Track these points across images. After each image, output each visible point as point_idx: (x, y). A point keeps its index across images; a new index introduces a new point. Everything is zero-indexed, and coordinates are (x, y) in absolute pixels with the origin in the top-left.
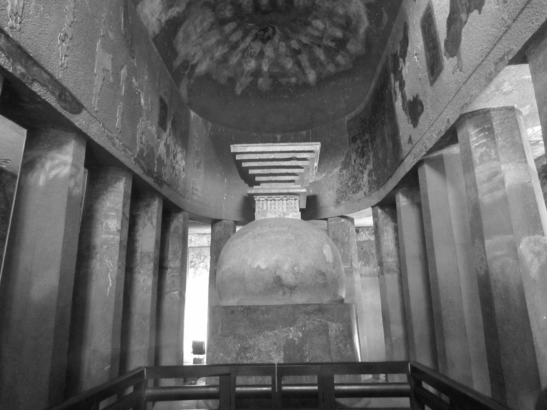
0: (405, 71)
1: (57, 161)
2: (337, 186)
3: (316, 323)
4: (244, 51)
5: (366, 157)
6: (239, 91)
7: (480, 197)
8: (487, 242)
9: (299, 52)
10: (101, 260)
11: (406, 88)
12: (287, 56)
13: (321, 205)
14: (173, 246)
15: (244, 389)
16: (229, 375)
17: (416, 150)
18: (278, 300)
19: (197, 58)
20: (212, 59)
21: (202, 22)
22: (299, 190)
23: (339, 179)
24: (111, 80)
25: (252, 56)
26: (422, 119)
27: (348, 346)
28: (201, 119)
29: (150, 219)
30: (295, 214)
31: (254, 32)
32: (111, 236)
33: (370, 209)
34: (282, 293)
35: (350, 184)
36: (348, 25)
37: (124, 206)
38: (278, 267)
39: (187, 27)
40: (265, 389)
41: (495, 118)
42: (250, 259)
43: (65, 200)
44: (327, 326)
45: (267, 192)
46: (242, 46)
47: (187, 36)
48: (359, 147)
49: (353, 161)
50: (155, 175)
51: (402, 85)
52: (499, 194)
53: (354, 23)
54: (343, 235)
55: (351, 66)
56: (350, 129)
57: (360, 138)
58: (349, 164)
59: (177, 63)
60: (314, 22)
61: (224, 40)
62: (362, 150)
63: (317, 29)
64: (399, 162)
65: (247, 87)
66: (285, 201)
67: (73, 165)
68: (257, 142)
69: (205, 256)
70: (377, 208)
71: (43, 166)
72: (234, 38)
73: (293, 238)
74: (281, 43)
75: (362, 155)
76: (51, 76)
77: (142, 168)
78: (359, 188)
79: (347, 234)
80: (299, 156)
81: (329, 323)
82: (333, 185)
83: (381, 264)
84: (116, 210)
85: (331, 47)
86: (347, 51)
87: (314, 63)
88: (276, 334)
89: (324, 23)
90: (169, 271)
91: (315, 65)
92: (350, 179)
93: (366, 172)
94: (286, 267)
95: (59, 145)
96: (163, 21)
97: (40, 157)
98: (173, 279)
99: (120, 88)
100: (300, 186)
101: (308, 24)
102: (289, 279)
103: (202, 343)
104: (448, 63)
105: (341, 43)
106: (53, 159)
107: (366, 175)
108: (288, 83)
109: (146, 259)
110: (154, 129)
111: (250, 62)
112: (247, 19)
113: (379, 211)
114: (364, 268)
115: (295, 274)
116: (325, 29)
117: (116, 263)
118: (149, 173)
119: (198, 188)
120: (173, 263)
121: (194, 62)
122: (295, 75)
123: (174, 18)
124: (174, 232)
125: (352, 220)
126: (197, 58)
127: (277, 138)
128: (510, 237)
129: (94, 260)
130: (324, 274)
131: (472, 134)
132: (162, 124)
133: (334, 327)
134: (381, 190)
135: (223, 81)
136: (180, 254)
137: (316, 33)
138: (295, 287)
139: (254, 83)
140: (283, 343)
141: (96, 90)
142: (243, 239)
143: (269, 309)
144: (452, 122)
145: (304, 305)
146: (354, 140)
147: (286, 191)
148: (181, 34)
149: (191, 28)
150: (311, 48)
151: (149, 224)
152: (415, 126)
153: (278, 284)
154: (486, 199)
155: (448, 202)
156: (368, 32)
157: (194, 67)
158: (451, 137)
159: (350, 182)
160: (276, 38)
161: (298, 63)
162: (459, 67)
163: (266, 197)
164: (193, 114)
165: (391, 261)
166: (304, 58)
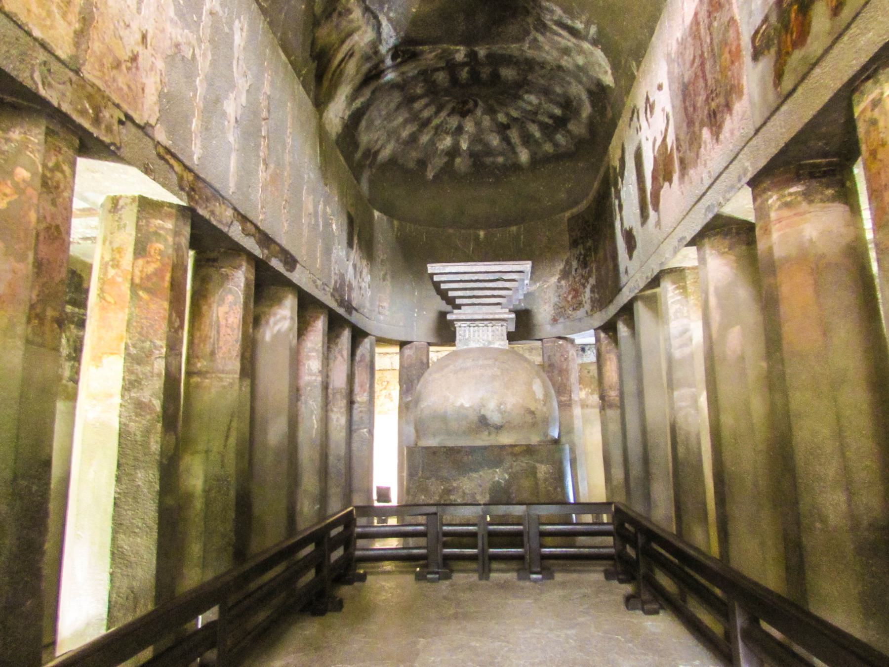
1: (278, 317)
2: (555, 299)
3: (524, 465)
4: (437, 128)
5: (588, 269)
6: (430, 175)
7: (672, 350)
8: (676, 394)
9: (506, 127)
10: (306, 402)
11: (624, 213)
12: (492, 131)
13: (535, 322)
14: (361, 376)
15: (450, 528)
16: (435, 514)
17: (631, 284)
18: (483, 440)
19: (380, 143)
20: (397, 140)
21: (388, 104)
22: (506, 316)
23: (556, 291)
24: (313, 222)
25: (447, 133)
26: (635, 253)
27: (559, 489)
28: (385, 218)
29: (340, 352)
30: (502, 343)
31: (450, 106)
32: (314, 378)
33: (592, 332)
34: (486, 433)
35: (569, 299)
36: (569, 105)
37: (323, 346)
38: (484, 406)
39: (373, 112)
40: (471, 528)
41: (689, 277)
42: (452, 397)
43: (288, 352)
44: (535, 468)
45: (469, 317)
46: (436, 122)
47: (371, 123)
48: (581, 254)
50: (346, 303)
51: (621, 207)
52: (687, 350)
53: (574, 103)
54: (561, 361)
55: (573, 148)
56: (571, 230)
57: (583, 243)
58: (569, 273)
59: (358, 155)
60: (526, 96)
61: (414, 117)
62: (584, 259)
63: (530, 103)
64: (617, 289)
65: (442, 168)
66: (490, 328)
67: (292, 318)
68: (460, 262)
69: (388, 382)
70: (600, 331)
71: (267, 323)
72: (426, 114)
73: (499, 373)
74: (485, 116)
75: (584, 264)
77: (336, 300)
78: (580, 304)
81: (538, 465)
82: (550, 298)
83: (602, 397)
84: (317, 351)
85: (547, 123)
86: (569, 132)
87: (527, 139)
89: (540, 100)
90: (356, 406)
91: (528, 142)
92: (569, 293)
95: (279, 301)
96: (346, 117)
97: (264, 313)
98: (361, 415)
99: (318, 225)
100: (507, 310)
101: (520, 97)
102: (495, 418)
103: (388, 489)
104: (652, 213)
105: (561, 123)
106: (275, 314)
108: (493, 163)
110: (342, 253)
111: (445, 139)
112: (443, 93)
113: (602, 335)
114: (590, 397)
115: (501, 412)
116: (540, 104)
117: (319, 404)
118: (341, 303)
119: (385, 304)
120: (361, 397)
121: (376, 149)
122: (501, 154)
123: (358, 110)
124: (360, 361)
125: (572, 341)
126: (380, 143)
127: (477, 237)
128: (694, 390)
129: (299, 403)
130: (532, 413)
131: (668, 290)
132: (350, 244)
133: (543, 470)
134: (603, 311)
135: (412, 165)
136: (368, 385)
137: (529, 108)
138: (501, 427)
139: (449, 164)
140: (489, 485)
141: (304, 240)
143: (473, 450)
144: (655, 273)
145: (512, 446)
146: (574, 244)
147: (491, 317)
148: (363, 123)
149: (376, 113)
150: (523, 122)
151: (340, 357)
152: (631, 257)
153: (483, 422)
154: (677, 354)
155: (658, 343)
156: (591, 118)
157: (377, 153)
158: (655, 282)
159: (570, 297)
160: (479, 112)
161: (506, 140)
162: (658, 223)
163: (468, 323)
164: (376, 214)
165: (613, 394)
166: (514, 135)
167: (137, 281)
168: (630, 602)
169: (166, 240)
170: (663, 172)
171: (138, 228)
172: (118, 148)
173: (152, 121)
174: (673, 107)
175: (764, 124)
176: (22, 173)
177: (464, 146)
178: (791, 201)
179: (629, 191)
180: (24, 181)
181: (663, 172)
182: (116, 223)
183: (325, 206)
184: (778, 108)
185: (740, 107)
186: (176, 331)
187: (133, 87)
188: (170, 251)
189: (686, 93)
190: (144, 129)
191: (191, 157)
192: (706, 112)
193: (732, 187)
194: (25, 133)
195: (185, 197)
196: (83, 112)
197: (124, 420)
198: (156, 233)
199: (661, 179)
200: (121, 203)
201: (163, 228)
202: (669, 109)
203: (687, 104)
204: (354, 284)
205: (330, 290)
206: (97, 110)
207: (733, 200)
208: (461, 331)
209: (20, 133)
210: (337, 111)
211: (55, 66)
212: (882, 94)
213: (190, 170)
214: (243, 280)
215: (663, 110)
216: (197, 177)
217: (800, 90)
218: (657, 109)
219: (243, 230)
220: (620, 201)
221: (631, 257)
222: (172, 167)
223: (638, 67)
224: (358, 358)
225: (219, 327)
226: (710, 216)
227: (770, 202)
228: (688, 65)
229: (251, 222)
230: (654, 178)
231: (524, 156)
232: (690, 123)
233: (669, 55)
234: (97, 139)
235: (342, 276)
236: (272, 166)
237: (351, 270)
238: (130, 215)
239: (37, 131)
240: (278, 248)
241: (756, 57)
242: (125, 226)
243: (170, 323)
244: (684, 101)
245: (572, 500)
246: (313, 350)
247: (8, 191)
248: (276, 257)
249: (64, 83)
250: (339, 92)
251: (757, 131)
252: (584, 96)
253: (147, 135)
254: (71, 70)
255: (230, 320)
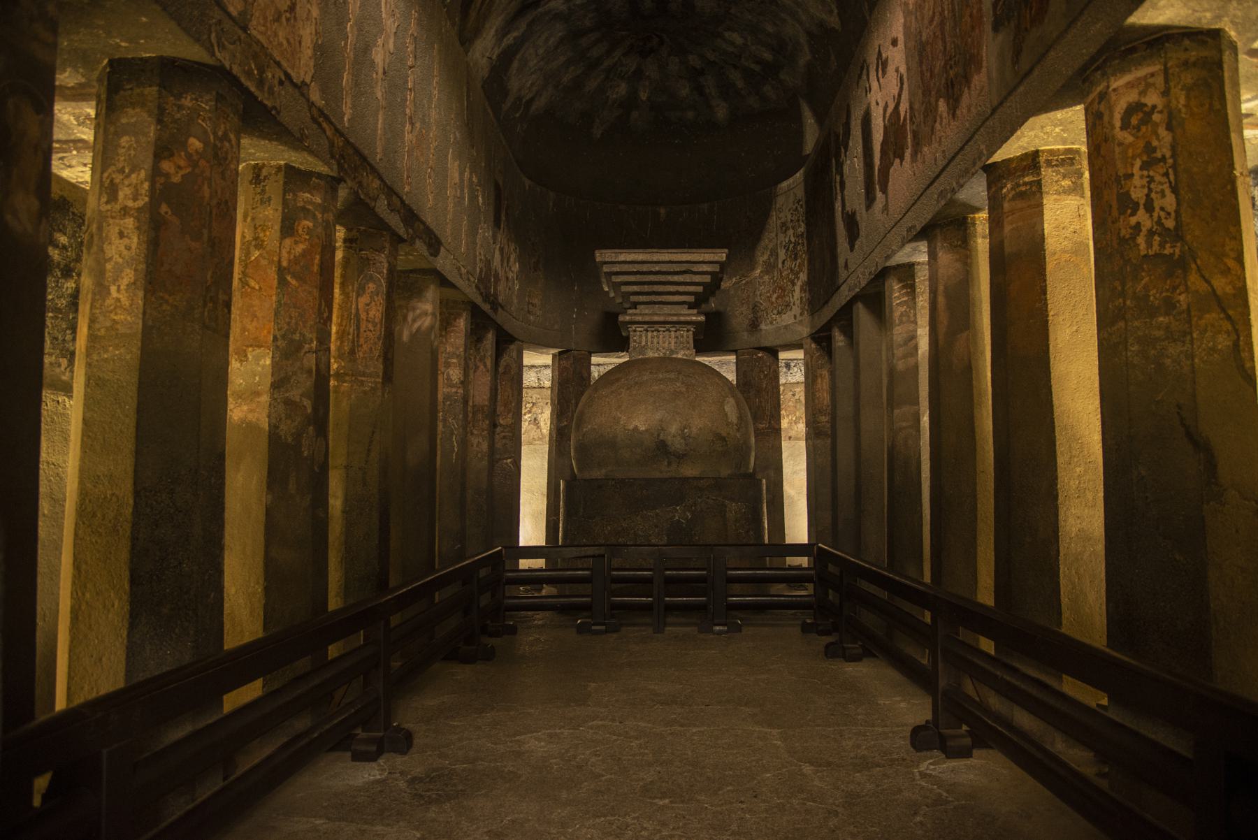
0: (846, 169)
1: (418, 312)
6: (597, 132)
8: (896, 412)
10: (445, 420)
11: (846, 193)
17: (851, 281)
18: (662, 470)
26: (858, 243)
29: (482, 359)
32: (454, 390)
45: (647, 319)
46: (607, 63)
49: (780, 262)
52: (911, 361)
58: (774, 266)
60: (727, 34)
63: (733, 44)
64: (835, 288)
67: (433, 314)
71: (405, 318)
76: (424, 223)
79: (766, 376)
80: (696, 268)
84: (458, 356)
88: (657, 514)
90: (498, 429)
92: (774, 292)
93: (799, 283)
94: (674, 429)
96: (494, 57)
102: (677, 444)
104: (879, 194)
106: (414, 309)
107: (797, 288)
109: (480, 416)
110: (489, 234)
118: (486, 298)
119: (536, 301)
130: (724, 439)
132: (497, 223)
133: (733, 509)
137: (731, 49)
138: (685, 455)
141: (450, 216)
142: (614, 388)
147: (675, 319)
148: (515, 64)
152: (852, 250)
153: (662, 448)
154: (900, 366)
162: (886, 208)
167: (285, 264)
168: (831, 652)
169: (314, 216)
170: (894, 147)
171: (285, 203)
172: (278, 113)
173: (308, 80)
174: (908, 69)
175: (1001, 103)
176: (195, 144)
177: (644, 96)
178: (1025, 192)
179: (853, 164)
180: (196, 151)
181: (894, 147)
182: (258, 197)
183: (471, 173)
184: (1015, 88)
185: (979, 80)
186: (325, 324)
187: (292, 40)
188: (319, 230)
189: (920, 52)
190: (301, 87)
191: (342, 121)
192: (943, 81)
193: (967, 171)
194: (196, 100)
195: (335, 167)
196: (249, 74)
197: (274, 421)
198: (304, 208)
199: (892, 156)
200: (264, 172)
201: (311, 203)
202: (903, 70)
203: (924, 67)
204: (501, 273)
205: (474, 280)
206: (262, 71)
207: (966, 186)
208: (639, 337)
209: (192, 100)
210: (484, 49)
211: (227, 25)
212: (1108, 87)
213: (342, 135)
214: (386, 265)
215: (897, 71)
216: (347, 141)
217: (1036, 73)
218: (891, 69)
219: (389, 204)
220: (842, 177)
221: (852, 249)
222: (324, 132)
223: (871, 10)
224: (501, 370)
225: (358, 321)
226: (943, 203)
227: (1005, 190)
228: (926, 22)
229: (398, 196)
230: (884, 152)
231: (721, 112)
232: (927, 92)
233: (906, 4)
234: (261, 103)
235: (488, 263)
236: (418, 125)
237: (497, 255)
238: (274, 187)
239: (208, 97)
240: (422, 227)
241: (996, 28)
242: (269, 199)
243: (320, 313)
244: (921, 63)
245: (766, 541)
246: (453, 355)
247: (182, 163)
248: (420, 238)
249: (234, 43)
250: (487, 26)
251: (994, 111)
252: (803, 39)
253: (303, 95)
254: (241, 28)
255: (371, 314)
